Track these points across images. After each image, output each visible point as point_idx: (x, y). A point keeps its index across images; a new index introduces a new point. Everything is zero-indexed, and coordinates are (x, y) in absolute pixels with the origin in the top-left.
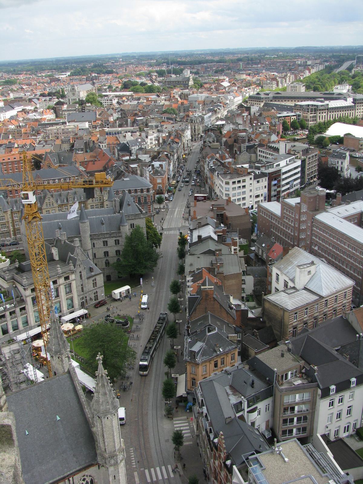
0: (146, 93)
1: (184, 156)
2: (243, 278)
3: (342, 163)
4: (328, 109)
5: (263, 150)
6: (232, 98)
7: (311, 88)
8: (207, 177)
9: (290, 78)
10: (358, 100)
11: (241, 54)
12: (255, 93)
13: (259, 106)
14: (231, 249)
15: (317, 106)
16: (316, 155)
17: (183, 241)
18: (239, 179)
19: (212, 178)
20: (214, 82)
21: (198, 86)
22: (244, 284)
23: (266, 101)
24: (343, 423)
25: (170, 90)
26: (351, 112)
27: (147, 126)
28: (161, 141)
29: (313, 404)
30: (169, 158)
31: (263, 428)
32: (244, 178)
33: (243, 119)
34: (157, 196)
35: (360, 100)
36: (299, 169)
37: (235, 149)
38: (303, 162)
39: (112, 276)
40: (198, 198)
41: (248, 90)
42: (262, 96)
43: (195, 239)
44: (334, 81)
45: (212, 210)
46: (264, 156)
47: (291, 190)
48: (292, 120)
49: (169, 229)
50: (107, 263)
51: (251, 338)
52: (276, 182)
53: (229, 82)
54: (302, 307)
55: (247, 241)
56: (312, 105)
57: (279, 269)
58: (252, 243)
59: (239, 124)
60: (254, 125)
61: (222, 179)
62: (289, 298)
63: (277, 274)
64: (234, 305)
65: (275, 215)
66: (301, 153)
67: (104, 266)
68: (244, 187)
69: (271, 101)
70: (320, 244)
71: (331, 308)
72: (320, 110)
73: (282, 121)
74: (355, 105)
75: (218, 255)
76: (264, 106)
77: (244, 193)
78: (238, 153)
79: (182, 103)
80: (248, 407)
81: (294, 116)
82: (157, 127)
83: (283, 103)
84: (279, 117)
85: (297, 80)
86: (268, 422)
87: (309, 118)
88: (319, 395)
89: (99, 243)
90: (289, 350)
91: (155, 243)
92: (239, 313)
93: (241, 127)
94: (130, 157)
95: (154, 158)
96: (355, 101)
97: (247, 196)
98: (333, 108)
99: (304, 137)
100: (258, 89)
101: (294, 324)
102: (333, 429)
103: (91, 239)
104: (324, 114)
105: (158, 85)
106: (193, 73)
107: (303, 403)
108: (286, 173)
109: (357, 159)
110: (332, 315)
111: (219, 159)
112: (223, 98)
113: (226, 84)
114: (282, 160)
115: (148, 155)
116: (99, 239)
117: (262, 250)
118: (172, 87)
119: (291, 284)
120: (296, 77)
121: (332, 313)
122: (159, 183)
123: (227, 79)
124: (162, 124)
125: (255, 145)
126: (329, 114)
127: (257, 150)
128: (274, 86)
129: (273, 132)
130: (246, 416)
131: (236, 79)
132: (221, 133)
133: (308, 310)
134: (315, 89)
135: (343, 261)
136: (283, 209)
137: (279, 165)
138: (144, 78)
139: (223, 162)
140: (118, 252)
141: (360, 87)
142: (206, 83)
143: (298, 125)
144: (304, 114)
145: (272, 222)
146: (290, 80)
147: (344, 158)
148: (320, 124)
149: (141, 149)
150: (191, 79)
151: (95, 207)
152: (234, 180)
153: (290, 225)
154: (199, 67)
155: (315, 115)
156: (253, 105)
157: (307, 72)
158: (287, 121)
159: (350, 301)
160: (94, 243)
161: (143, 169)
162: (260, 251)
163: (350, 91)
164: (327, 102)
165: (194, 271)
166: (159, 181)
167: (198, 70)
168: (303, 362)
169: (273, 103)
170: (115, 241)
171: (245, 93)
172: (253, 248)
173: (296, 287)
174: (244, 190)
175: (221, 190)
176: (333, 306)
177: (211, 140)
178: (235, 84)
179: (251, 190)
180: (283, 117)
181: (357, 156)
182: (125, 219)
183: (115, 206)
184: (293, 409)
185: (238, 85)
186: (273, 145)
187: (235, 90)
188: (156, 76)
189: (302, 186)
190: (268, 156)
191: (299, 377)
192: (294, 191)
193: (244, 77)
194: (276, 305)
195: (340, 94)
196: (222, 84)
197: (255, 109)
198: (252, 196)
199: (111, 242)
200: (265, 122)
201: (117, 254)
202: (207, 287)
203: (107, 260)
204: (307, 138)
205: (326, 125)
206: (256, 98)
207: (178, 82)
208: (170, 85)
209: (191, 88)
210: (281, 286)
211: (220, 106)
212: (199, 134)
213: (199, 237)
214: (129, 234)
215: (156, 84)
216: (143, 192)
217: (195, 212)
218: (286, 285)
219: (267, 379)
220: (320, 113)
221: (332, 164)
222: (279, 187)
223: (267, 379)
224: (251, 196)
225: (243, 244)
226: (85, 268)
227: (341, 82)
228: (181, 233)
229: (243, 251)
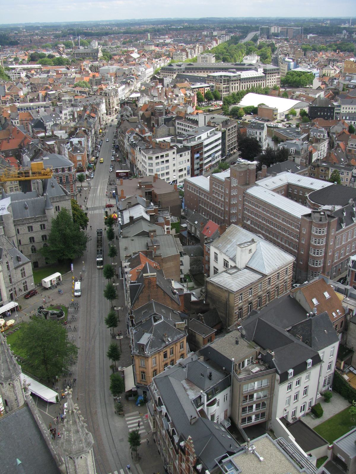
0: (55, 65)
1: (101, 131)
2: (181, 259)
3: (260, 134)
4: (240, 80)
6: (144, 70)
7: (220, 59)
8: (127, 153)
9: (198, 49)
10: (268, 70)
11: (147, 25)
12: (166, 64)
13: (171, 77)
14: (164, 228)
15: (230, 77)
16: (235, 127)
17: (110, 221)
18: (162, 154)
19: (133, 153)
20: (123, 53)
21: (107, 58)
22: (182, 265)
23: (178, 72)
24: (300, 404)
25: (79, 62)
26: (262, 82)
27: (59, 100)
28: (76, 116)
29: (271, 390)
30: (87, 134)
31: (222, 417)
32: (167, 153)
33: (158, 91)
34: (79, 174)
35: (270, 70)
36: (220, 141)
37: (153, 122)
39: (39, 263)
40: (119, 174)
41: (159, 62)
42: (175, 67)
43: (127, 221)
44: (241, 51)
45: (140, 188)
47: (213, 163)
48: (206, 91)
49: (94, 209)
50: (34, 250)
51: (197, 323)
52: (198, 155)
53: (138, 53)
54: (246, 287)
55: (178, 219)
56: (225, 76)
57: (217, 248)
58: (182, 220)
59: (154, 97)
60: (169, 96)
61: (145, 155)
62: (233, 279)
63: (215, 253)
64: (176, 289)
65: (204, 190)
67: (30, 253)
68: (167, 161)
69: (184, 72)
70: (253, 218)
71: (274, 286)
72: (233, 81)
73: (196, 93)
74: (265, 76)
75: (153, 236)
76: (176, 77)
77: (168, 167)
78: (156, 126)
79: (93, 75)
80: (208, 400)
82: (70, 101)
83: (196, 74)
85: (206, 51)
86: (226, 412)
87: (222, 89)
88: (277, 380)
89: (24, 229)
90: (242, 336)
91: (81, 225)
92: (182, 298)
93: (156, 100)
94: (45, 134)
95: (72, 134)
96: (265, 71)
97: (170, 170)
98: (245, 79)
99: (218, 108)
100: (169, 61)
101: (240, 305)
102: (290, 410)
103: (15, 226)
105: (67, 57)
106: (101, 44)
107: (261, 389)
108: (207, 145)
109: (272, 129)
110: (274, 292)
111: (139, 133)
112: (135, 70)
113: (135, 55)
114: (203, 132)
115: (64, 131)
116: (23, 224)
117: (195, 228)
118: (81, 59)
119: (231, 263)
120: (204, 47)
121: (274, 290)
122: (80, 161)
123: (136, 50)
124: (76, 98)
125: (172, 117)
126: (241, 84)
127: (175, 123)
128: (184, 57)
130: (205, 410)
131: (145, 50)
132: (137, 106)
133: (253, 290)
134: (224, 60)
135: (277, 235)
137: (200, 138)
138: (51, 49)
139: (143, 136)
140: (44, 237)
141: (267, 58)
142: (115, 55)
143: (212, 96)
144: (217, 85)
146: (198, 51)
147: (262, 128)
148: (233, 94)
149: (56, 125)
150: (100, 51)
151: (14, 189)
152: (157, 155)
153: (220, 200)
154: (106, 38)
155: (228, 85)
156: (166, 77)
157: (214, 42)
158: (202, 92)
159: (290, 277)
160: (18, 230)
161: (61, 146)
162: (193, 229)
163: (259, 61)
164: (238, 73)
165: (130, 256)
166: (79, 158)
167: (106, 41)
168: (258, 349)
169: (186, 74)
170: (41, 225)
171: (156, 65)
172: (184, 225)
173: (237, 266)
174: (167, 164)
175: (144, 165)
176: (275, 283)
177: (128, 114)
178: (145, 55)
180: (197, 88)
181: (272, 126)
182: (49, 201)
183: (38, 188)
184: (252, 396)
185: (147, 56)
187: (145, 61)
188: (63, 47)
189: (224, 158)
191: (256, 363)
192: (216, 163)
193: (153, 48)
194: (220, 287)
195: (251, 65)
196: (132, 55)
197: (168, 80)
198: (176, 171)
199: (36, 226)
200: (180, 93)
201: (43, 240)
202: (149, 274)
203: (33, 246)
204: (222, 108)
205: (240, 96)
206: (168, 70)
207: (87, 53)
208: (79, 57)
209: (100, 60)
210: (220, 266)
211: (133, 78)
212: (113, 107)
213: (131, 218)
214: (55, 217)
215: (65, 56)
216: (64, 171)
217: (122, 191)
218: (226, 264)
219: (224, 368)
221: (251, 135)
222: (202, 160)
223: (224, 368)
225: (175, 222)
226: (12, 258)
227: (249, 53)
228: (106, 212)
229: (175, 229)
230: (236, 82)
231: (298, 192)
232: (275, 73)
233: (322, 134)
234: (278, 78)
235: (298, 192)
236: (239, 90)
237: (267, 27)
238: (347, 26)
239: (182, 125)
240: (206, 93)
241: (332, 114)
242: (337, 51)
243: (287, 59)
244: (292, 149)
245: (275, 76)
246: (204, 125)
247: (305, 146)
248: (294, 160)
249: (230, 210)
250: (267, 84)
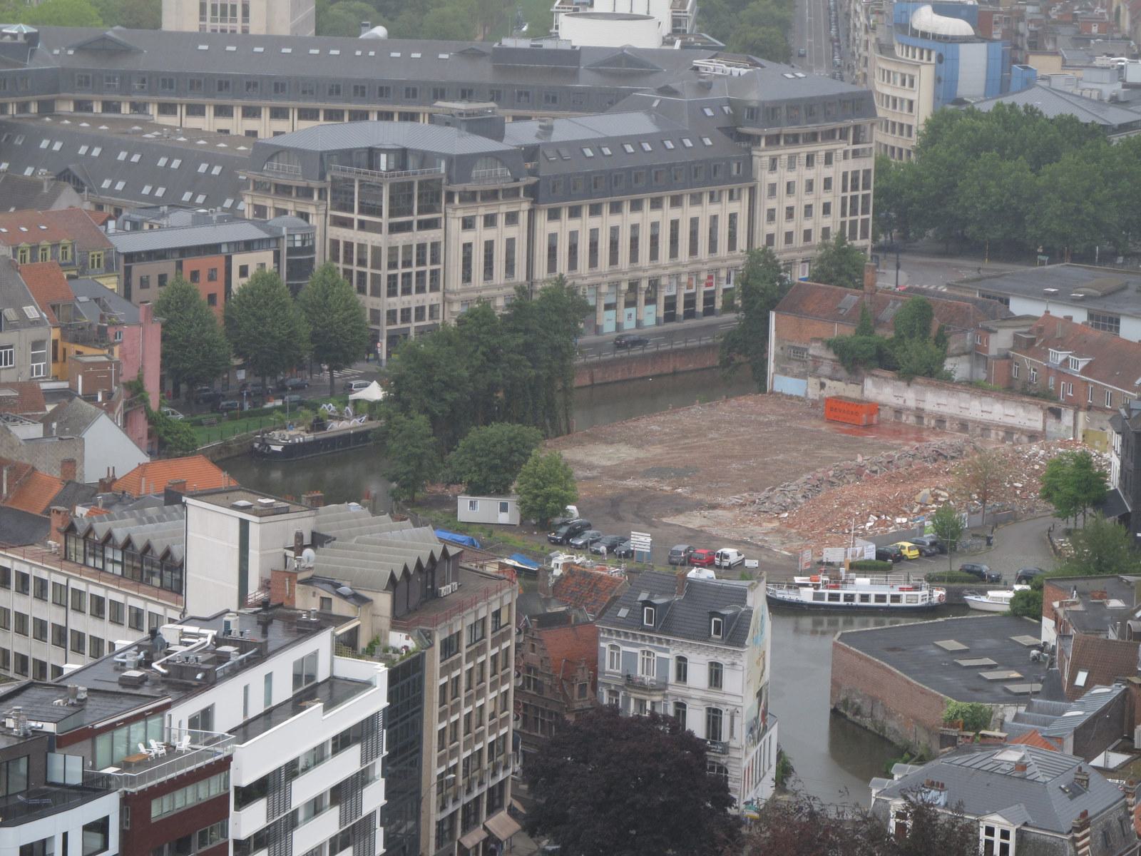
5: (33, 572)
46: (41, 626)
66: (383, 602)
73: (154, 293)
81: (248, 246)
84: (130, 257)
104: (501, 233)
129: (90, 398)
155: (429, 236)
158: (204, 288)
190: (82, 623)
220: (468, 224)
221: (630, 682)
230: (502, 209)
232: (829, 135)
234: (852, 181)
236: (520, 275)
239: (41, 595)
240: (243, 290)
244: (997, 821)
245: (828, 160)
246: (233, 604)
250: (764, 228)
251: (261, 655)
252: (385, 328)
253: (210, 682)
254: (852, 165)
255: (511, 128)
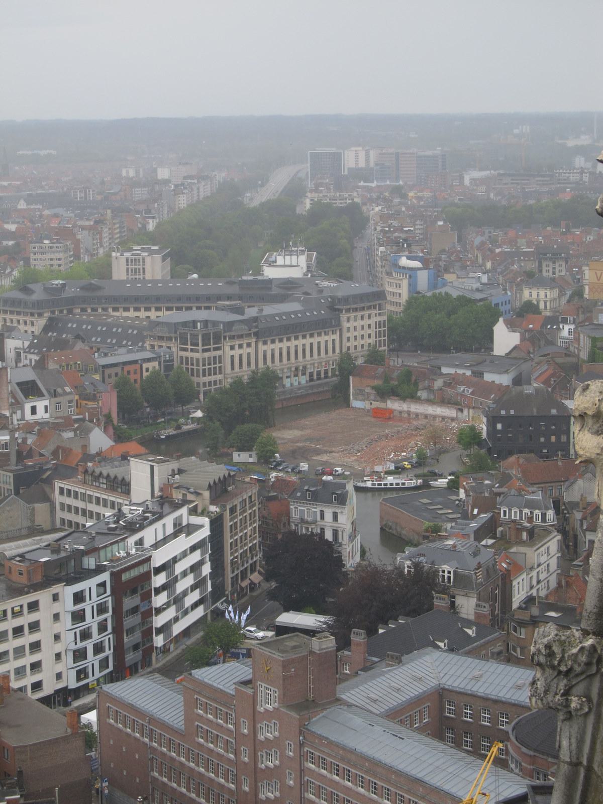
3: (335, 517)
5: (73, 489)
23: (53, 312)
38: (217, 524)
46: (77, 509)
66: (207, 494)
73: (114, 379)
76: (46, 329)
81: (149, 360)
84: (104, 367)
104: (245, 351)
129: (91, 421)
136: (190, 705)
145: (154, 750)
155: (218, 353)
158: (132, 377)
179: (57, 637)
186: (106, 470)
190: (92, 507)
220: (232, 348)
221: (303, 521)
224: (58, 656)
230: (245, 342)
231: (476, 716)
232: (369, 308)
233: (537, 512)
234: (379, 325)
235: (476, 716)
236: (253, 367)
237: (334, 150)
238: (584, 140)
239: (76, 497)
240: (147, 377)
241: (564, 438)
242: (563, 223)
243: (404, 262)
244: (446, 567)
245: (369, 317)
246: (149, 497)
247: (486, 556)
248: (453, 603)
249: (255, 790)
250: (346, 344)
251: (160, 517)
252: (202, 389)
253: (142, 528)
254: (378, 319)
255: (247, 310)
